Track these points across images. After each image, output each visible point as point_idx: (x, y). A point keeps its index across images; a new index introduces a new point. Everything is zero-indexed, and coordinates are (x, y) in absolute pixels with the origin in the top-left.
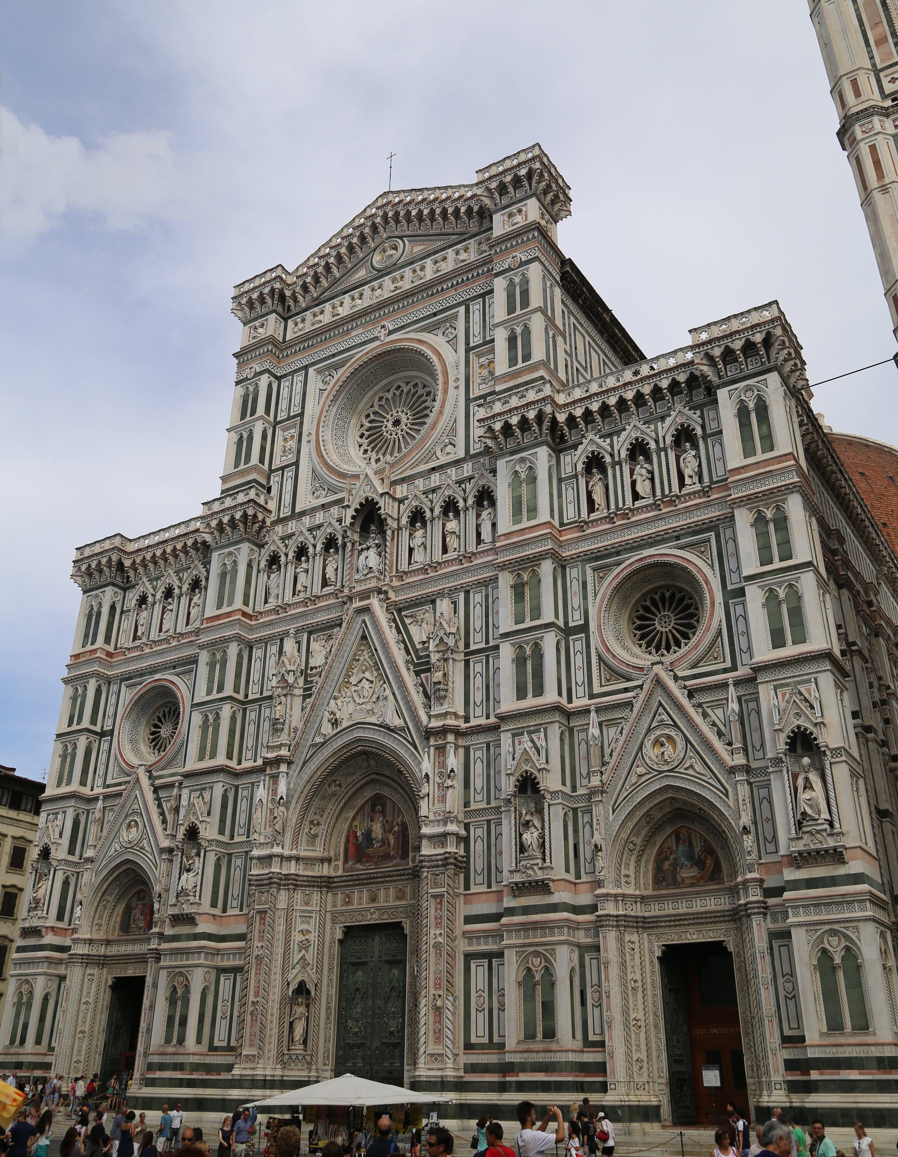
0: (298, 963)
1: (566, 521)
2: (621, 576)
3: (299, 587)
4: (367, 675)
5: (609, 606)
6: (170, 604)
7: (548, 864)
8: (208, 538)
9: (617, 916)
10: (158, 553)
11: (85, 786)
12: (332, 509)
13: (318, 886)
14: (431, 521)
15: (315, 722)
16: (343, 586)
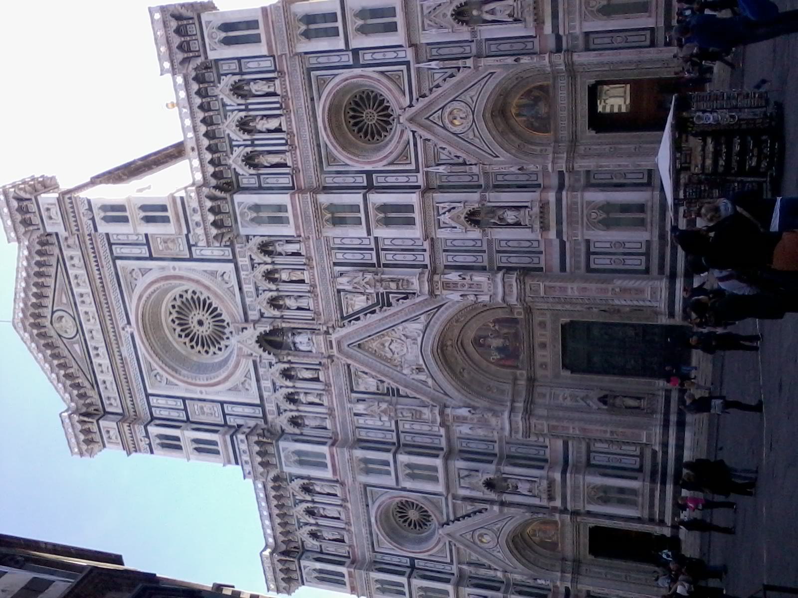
0: (586, 402)
1: (291, 185)
2: (335, 144)
3: (317, 401)
4: (387, 344)
5: (354, 154)
6: (319, 511)
8: (272, 475)
14: (280, 291)
16: (320, 364)
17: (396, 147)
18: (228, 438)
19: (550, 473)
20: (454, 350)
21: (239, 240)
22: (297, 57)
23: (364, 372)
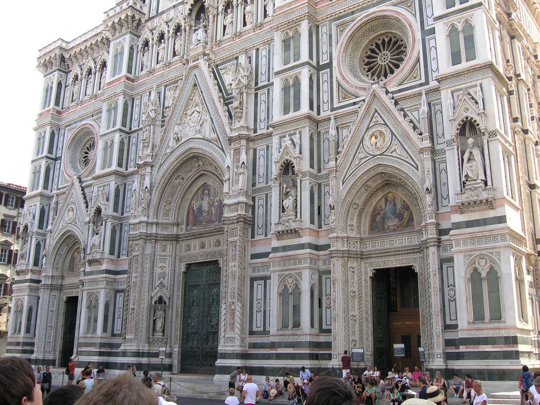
0: (158, 286)
4: (197, 109)
9: (343, 251)
11: (47, 189)
12: (179, 8)
13: (170, 240)
14: (237, 7)
15: (166, 140)
17: (352, 86)
20: (197, 169)
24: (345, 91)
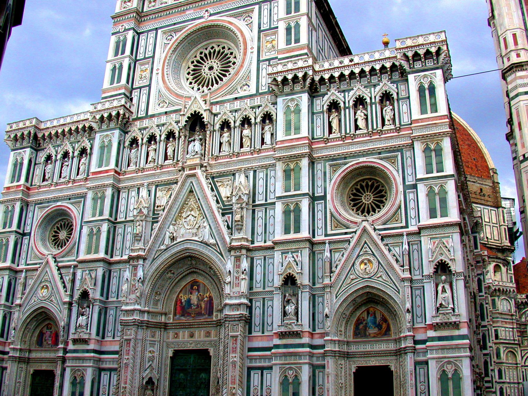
0: (148, 368)
1: (315, 137)
2: (346, 171)
3: (150, 159)
4: (192, 213)
5: (339, 186)
6: (66, 161)
7: (300, 323)
8: (94, 125)
9: (335, 351)
10: (60, 131)
12: (172, 115)
13: (159, 328)
14: (234, 129)
16: (178, 161)
17: (344, 218)
18: (123, 91)
19: (93, 341)
21: (273, 97)
22: (411, 141)
23: (171, 195)
24: (338, 221)
